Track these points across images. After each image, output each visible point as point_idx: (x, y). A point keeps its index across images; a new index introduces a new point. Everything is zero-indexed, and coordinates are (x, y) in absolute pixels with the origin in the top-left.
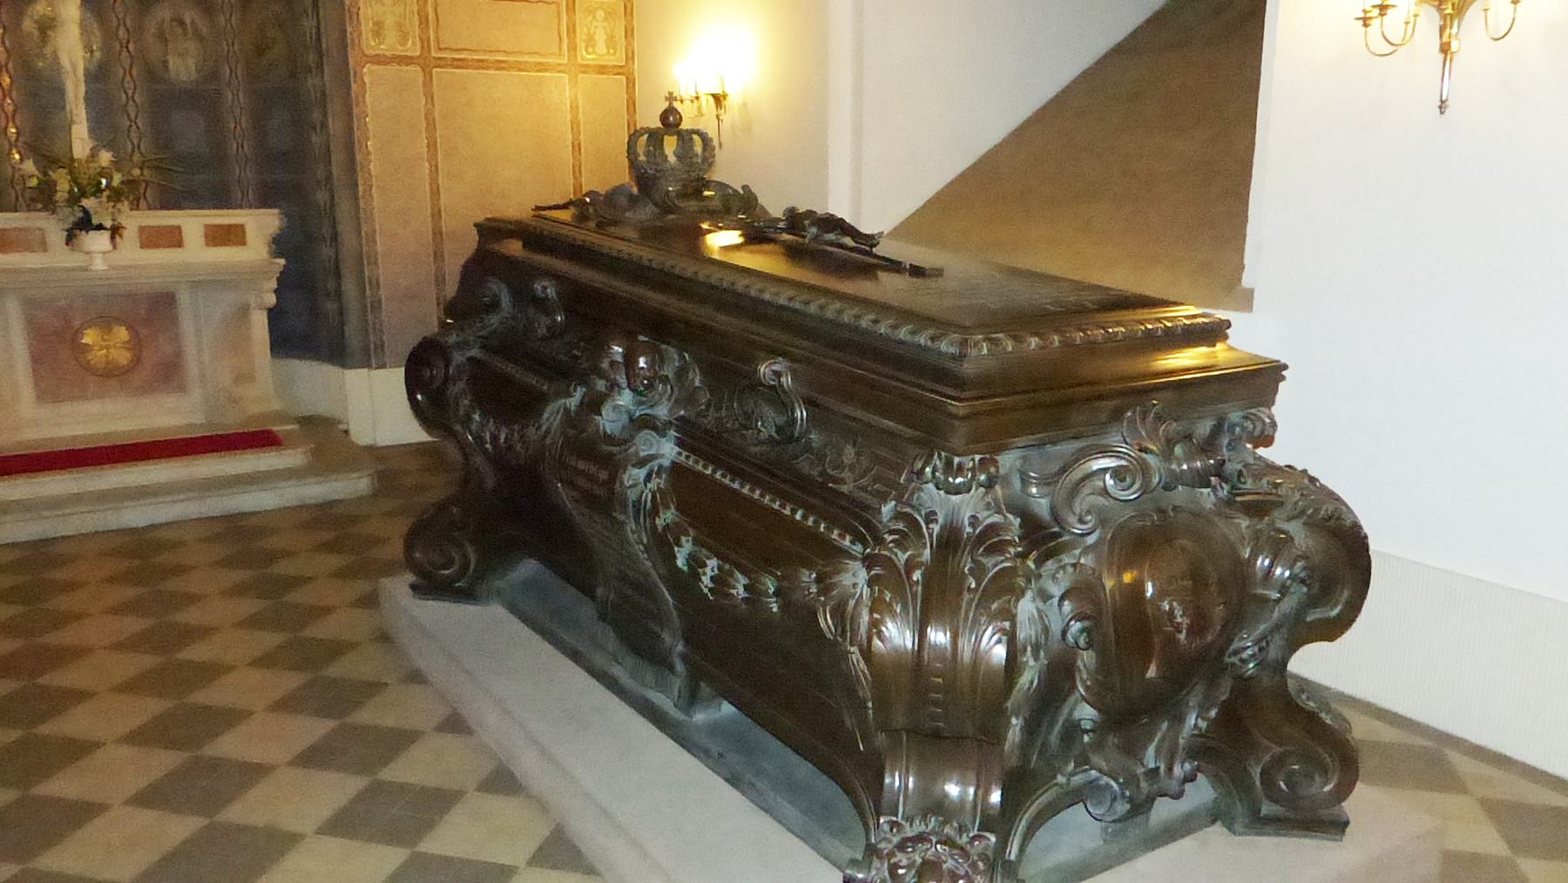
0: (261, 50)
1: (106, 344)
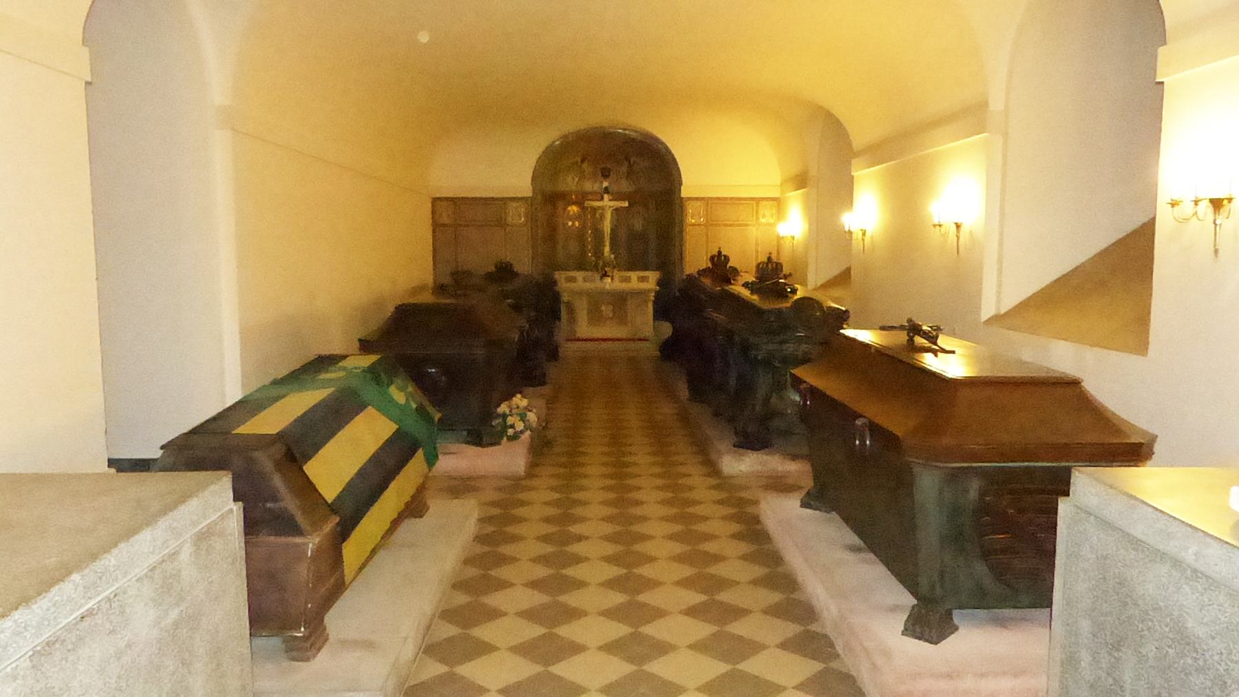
1: (606, 310)
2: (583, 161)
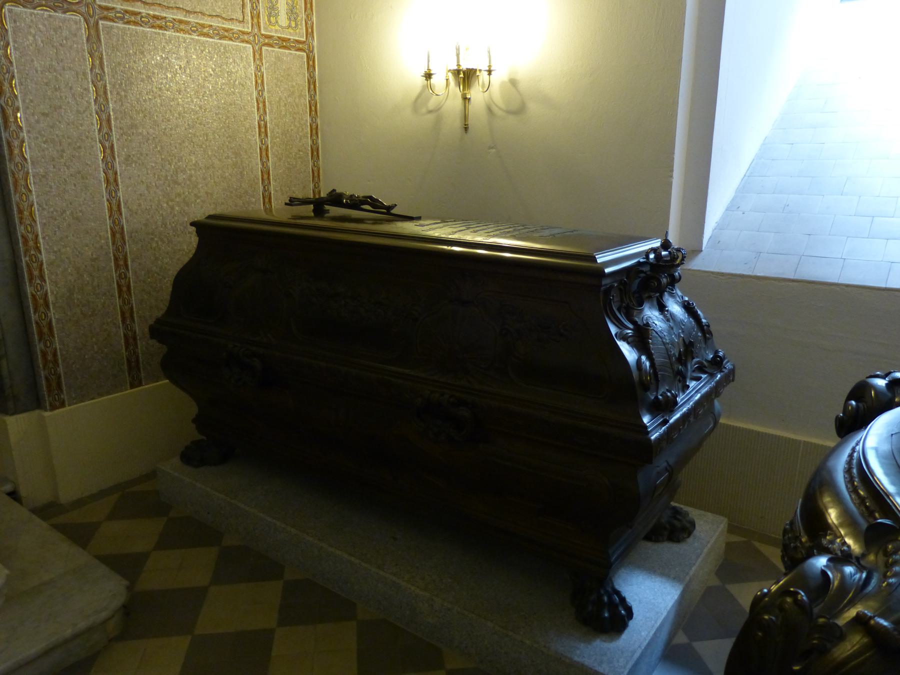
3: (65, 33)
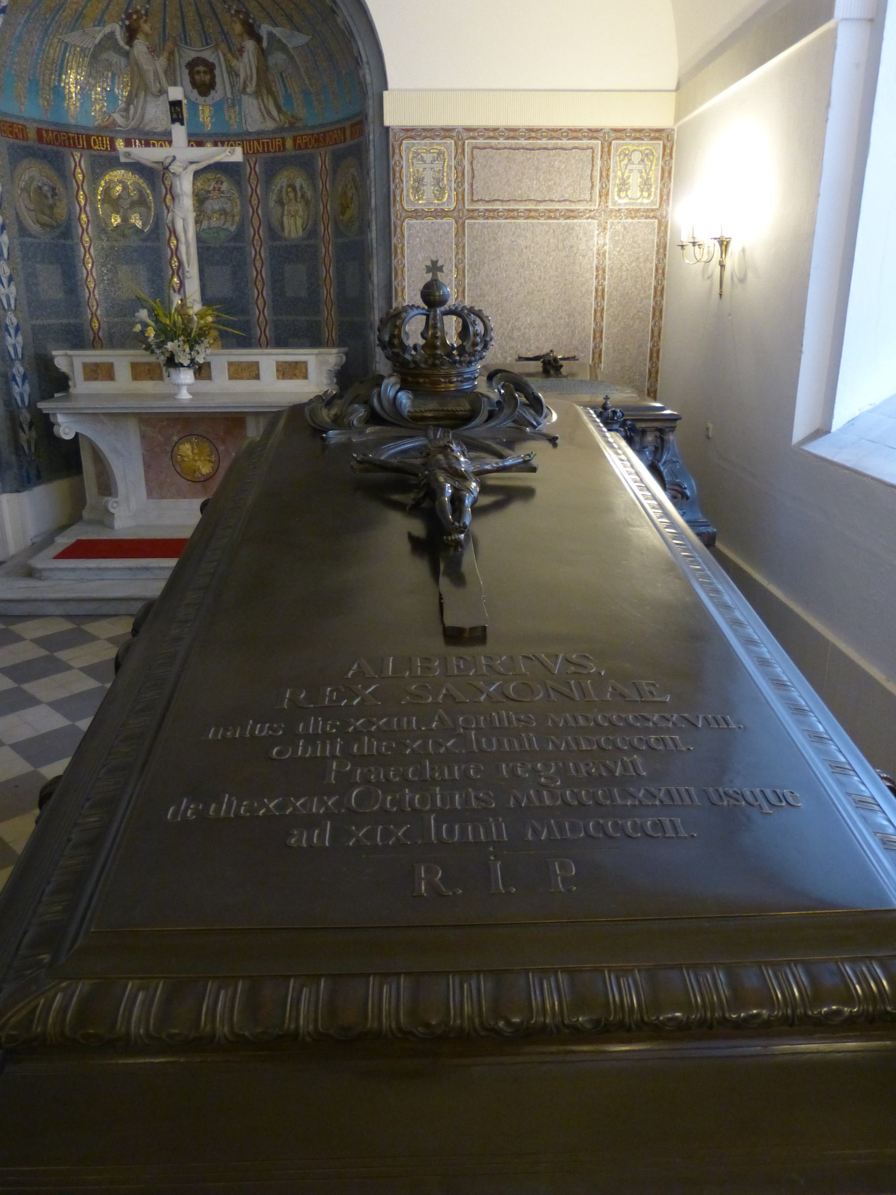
0: (344, 209)
2: (131, 33)
3: (441, 232)
